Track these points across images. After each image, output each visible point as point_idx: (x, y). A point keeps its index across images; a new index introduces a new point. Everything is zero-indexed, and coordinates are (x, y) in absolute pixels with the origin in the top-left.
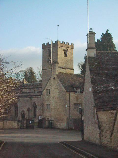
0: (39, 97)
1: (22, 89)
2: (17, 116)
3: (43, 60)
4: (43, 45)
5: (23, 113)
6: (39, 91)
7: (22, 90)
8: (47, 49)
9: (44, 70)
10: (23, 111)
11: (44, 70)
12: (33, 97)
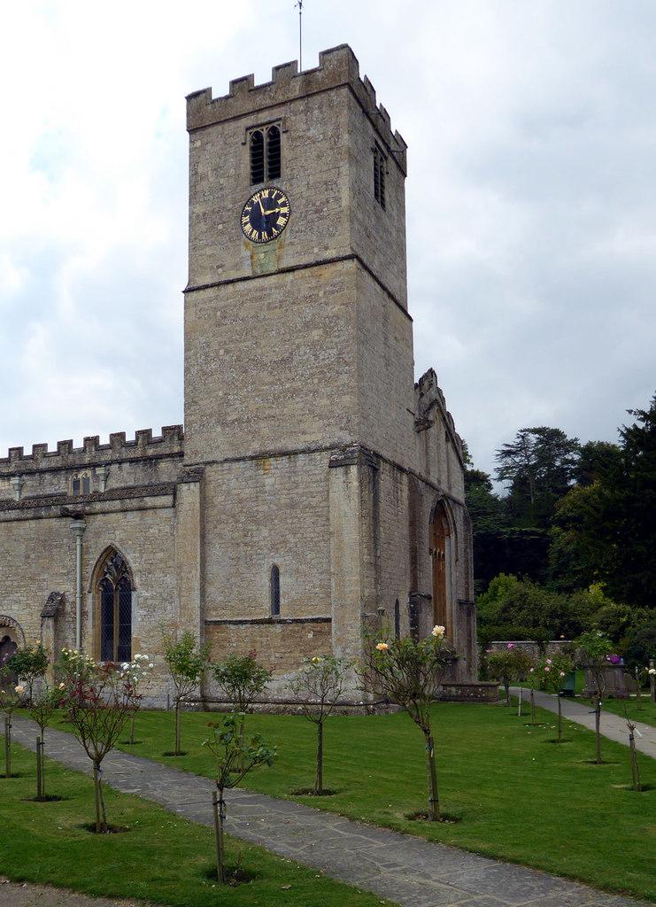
3: (194, 220)
4: (198, 100)
8: (233, 125)
9: (206, 287)
11: (210, 292)
12: (98, 506)
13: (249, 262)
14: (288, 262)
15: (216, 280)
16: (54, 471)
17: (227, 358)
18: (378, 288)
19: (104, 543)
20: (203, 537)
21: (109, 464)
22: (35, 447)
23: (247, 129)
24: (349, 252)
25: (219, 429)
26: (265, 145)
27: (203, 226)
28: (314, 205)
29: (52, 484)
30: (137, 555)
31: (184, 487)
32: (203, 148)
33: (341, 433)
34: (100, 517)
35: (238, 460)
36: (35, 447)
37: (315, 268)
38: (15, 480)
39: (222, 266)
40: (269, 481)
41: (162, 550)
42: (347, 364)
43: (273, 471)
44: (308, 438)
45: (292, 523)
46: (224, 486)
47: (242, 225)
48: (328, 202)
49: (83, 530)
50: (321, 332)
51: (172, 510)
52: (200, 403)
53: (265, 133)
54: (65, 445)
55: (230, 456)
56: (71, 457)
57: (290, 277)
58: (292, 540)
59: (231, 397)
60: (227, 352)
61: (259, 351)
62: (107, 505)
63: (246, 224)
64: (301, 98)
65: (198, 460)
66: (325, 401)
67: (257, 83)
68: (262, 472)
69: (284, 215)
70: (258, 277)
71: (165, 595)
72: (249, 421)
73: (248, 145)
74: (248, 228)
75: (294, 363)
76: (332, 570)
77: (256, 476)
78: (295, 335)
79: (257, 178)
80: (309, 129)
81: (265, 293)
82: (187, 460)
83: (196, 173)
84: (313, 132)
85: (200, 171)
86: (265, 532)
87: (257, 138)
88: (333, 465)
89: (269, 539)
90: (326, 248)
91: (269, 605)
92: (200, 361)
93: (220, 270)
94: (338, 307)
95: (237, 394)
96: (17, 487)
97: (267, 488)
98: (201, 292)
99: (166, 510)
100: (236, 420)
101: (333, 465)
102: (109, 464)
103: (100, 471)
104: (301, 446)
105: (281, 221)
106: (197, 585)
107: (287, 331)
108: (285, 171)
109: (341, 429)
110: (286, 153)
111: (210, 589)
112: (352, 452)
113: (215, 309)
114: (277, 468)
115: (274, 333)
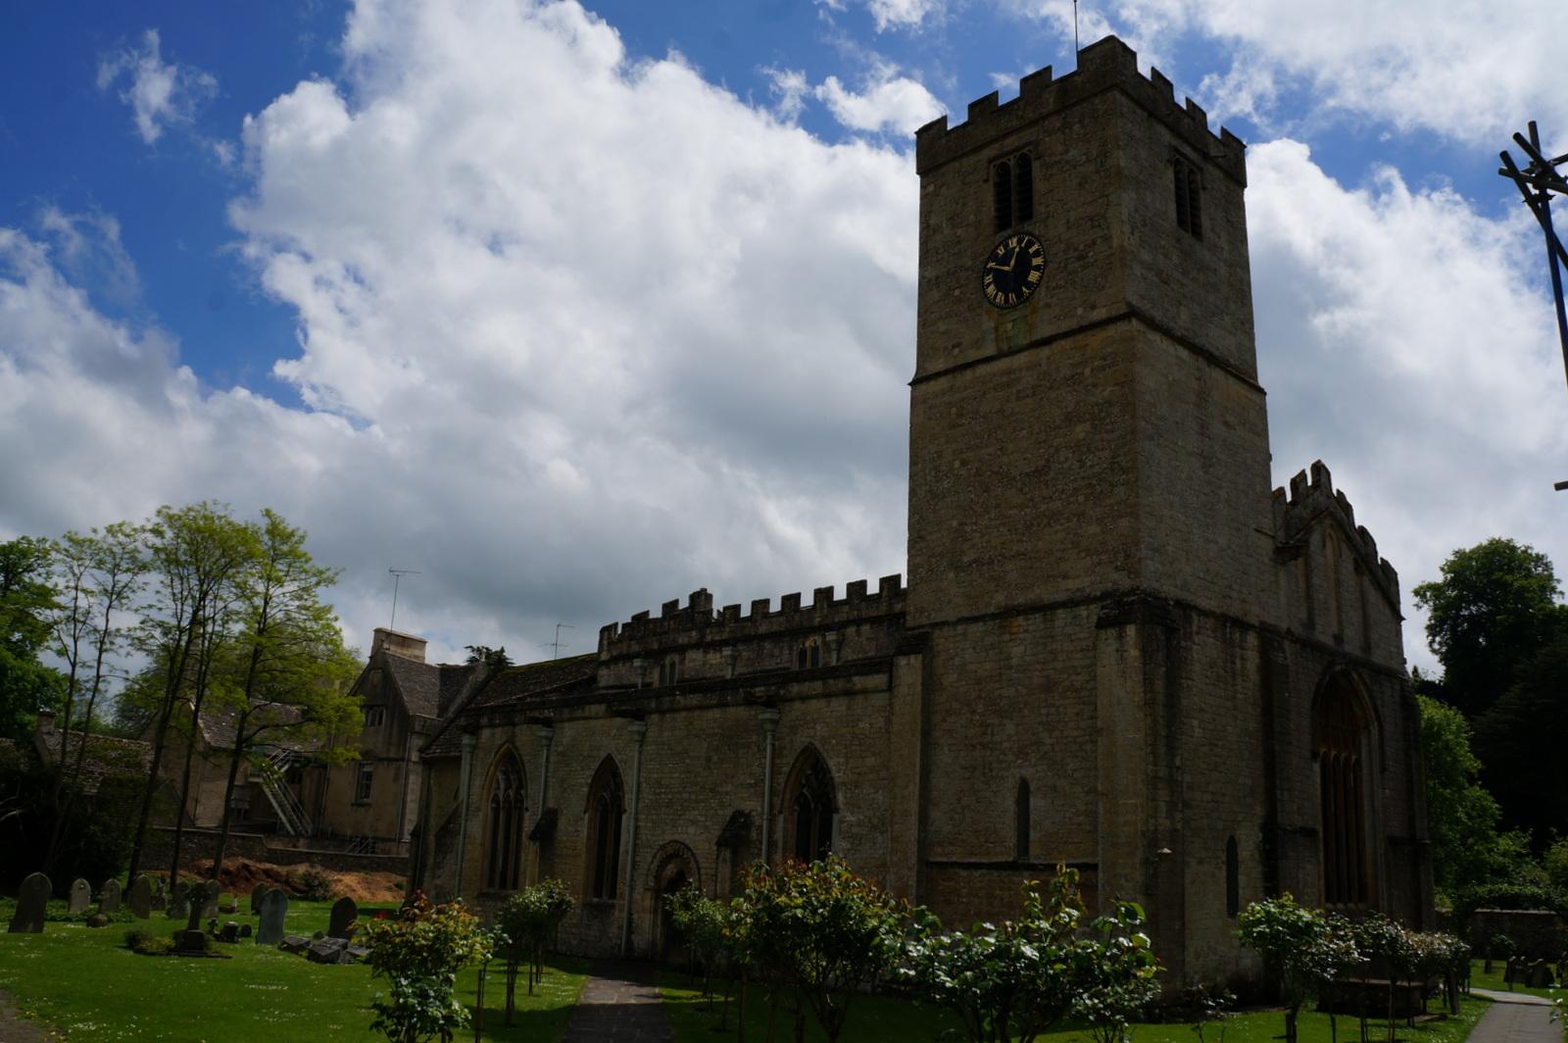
0: (865, 692)
1: (682, 650)
2: (613, 895)
5: (671, 869)
6: (849, 654)
7: (676, 658)
8: (972, 159)
9: (938, 375)
10: (677, 853)
11: (943, 383)
12: (795, 688)
13: (993, 336)
14: (1045, 330)
15: (951, 364)
16: (775, 637)
17: (963, 472)
18: (1184, 353)
19: (801, 740)
20: (926, 735)
21: (844, 625)
22: (754, 604)
23: (990, 161)
24: (1123, 309)
25: (951, 575)
26: (1012, 178)
27: (935, 295)
28: (1076, 250)
29: (772, 656)
30: (842, 760)
31: (902, 661)
32: (936, 194)
33: (1116, 576)
34: (797, 705)
35: (975, 620)
36: (754, 604)
37: (1079, 337)
38: (727, 651)
39: (958, 345)
40: (1016, 651)
41: (874, 754)
42: (1124, 471)
43: (1021, 636)
45: (1048, 715)
46: (957, 659)
47: (984, 287)
48: (1094, 243)
49: (775, 722)
50: (1087, 426)
51: (886, 695)
52: (928, 538)
53: (1012, 163)
54: (791, 601)
55: (966, 614)
56: (797, 618)
57: (1045, 352)
58: (1048, 741)
59: (968, 528)
60: (964, 463)
61: (1005, 459)
62: (806, 687)
63: (989, 284)
64: (1057, 112)
65: (925, 621)
66: (1094, 529)
67: (1002, 101)
68: (1007, 637)
69: (1037, 268)
70: (1006, 355)
71: (875, 821)
72: (991, 562)
73: (991, 183)
74: (991, 290)
75: (1052, 474)
76: (1100, 788)
77: (999, 643)
78: (1053, 433)
79: (1003, 222)
80: (1067, 151)
81: (1013, 376)
82: (910, 622)
83: (928, 226)
84: (1073, 153)
85: (932, 222)
86: (1010, 728)
87: (1004, 170)
88: (1102, 624)
89: (1015, 738)
90: (1093, 307)
91: (1014, 840)
92: (929, 478)
93: (956, 351)
94: (1109, 389)
95: (976, 523)
96: (729, 661)
97: (1014, 662)
98: (932, 383)
99: (882, 694)
100: (975, 561)
101: (1102, 624)
102: (844, 625)
103: (831, 637)
104: (1061, 597)
105: (1033, 276)
106: (914, 806)
107: (1043, 428)
108: (1039, 209)
109: (1117, 568)
110: (1039, 186)
111: (936, 814)
112: (1132, 603)
114: (1026, 631)
115: (1025, 432)
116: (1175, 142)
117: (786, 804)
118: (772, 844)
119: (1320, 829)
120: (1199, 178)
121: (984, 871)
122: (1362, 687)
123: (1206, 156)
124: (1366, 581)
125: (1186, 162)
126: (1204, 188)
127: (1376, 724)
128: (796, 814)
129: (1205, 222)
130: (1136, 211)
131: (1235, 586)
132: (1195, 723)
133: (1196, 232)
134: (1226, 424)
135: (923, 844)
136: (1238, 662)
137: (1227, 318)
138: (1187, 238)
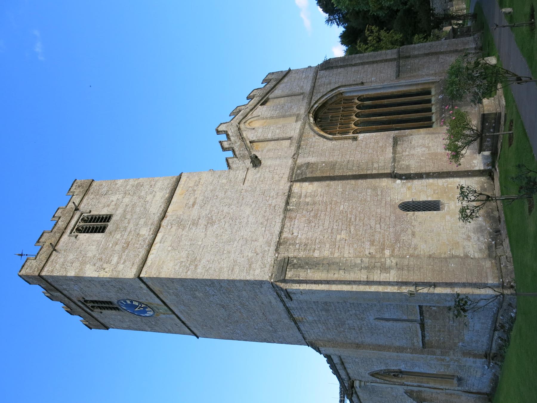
32: (114, 325)
44: (273, 301)
69: (132, 302)
90: (141, 287)
104: (281, 305)
113: (203, 329)
116: (68, 231)
117: (399, 381)
118: (420, 386)
119: (393, 133)
120: (86, 215)
121: (426, 332)
122: (322, 100)
123: (77, 209)
124: (271, 96)
125: (78, 224)
126: (90, 212)
127: (339, 89)
128: (403, 376)
129: (104, 212)
130: (94, 265)
131: (270, 202)
132: (339, 237)
133: (107, 218)
134: (193, 205)
135: (414, 351)
136: (307, 200)
137: (147, 199)
138: (110, 226)
